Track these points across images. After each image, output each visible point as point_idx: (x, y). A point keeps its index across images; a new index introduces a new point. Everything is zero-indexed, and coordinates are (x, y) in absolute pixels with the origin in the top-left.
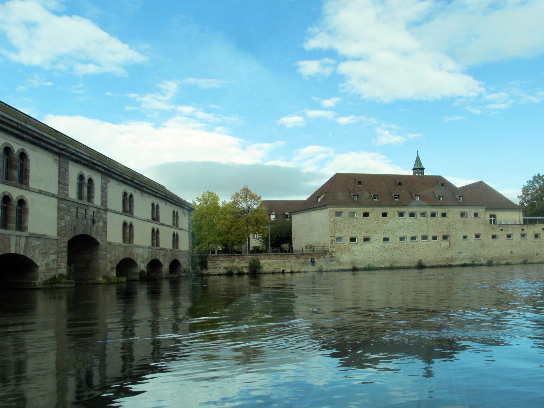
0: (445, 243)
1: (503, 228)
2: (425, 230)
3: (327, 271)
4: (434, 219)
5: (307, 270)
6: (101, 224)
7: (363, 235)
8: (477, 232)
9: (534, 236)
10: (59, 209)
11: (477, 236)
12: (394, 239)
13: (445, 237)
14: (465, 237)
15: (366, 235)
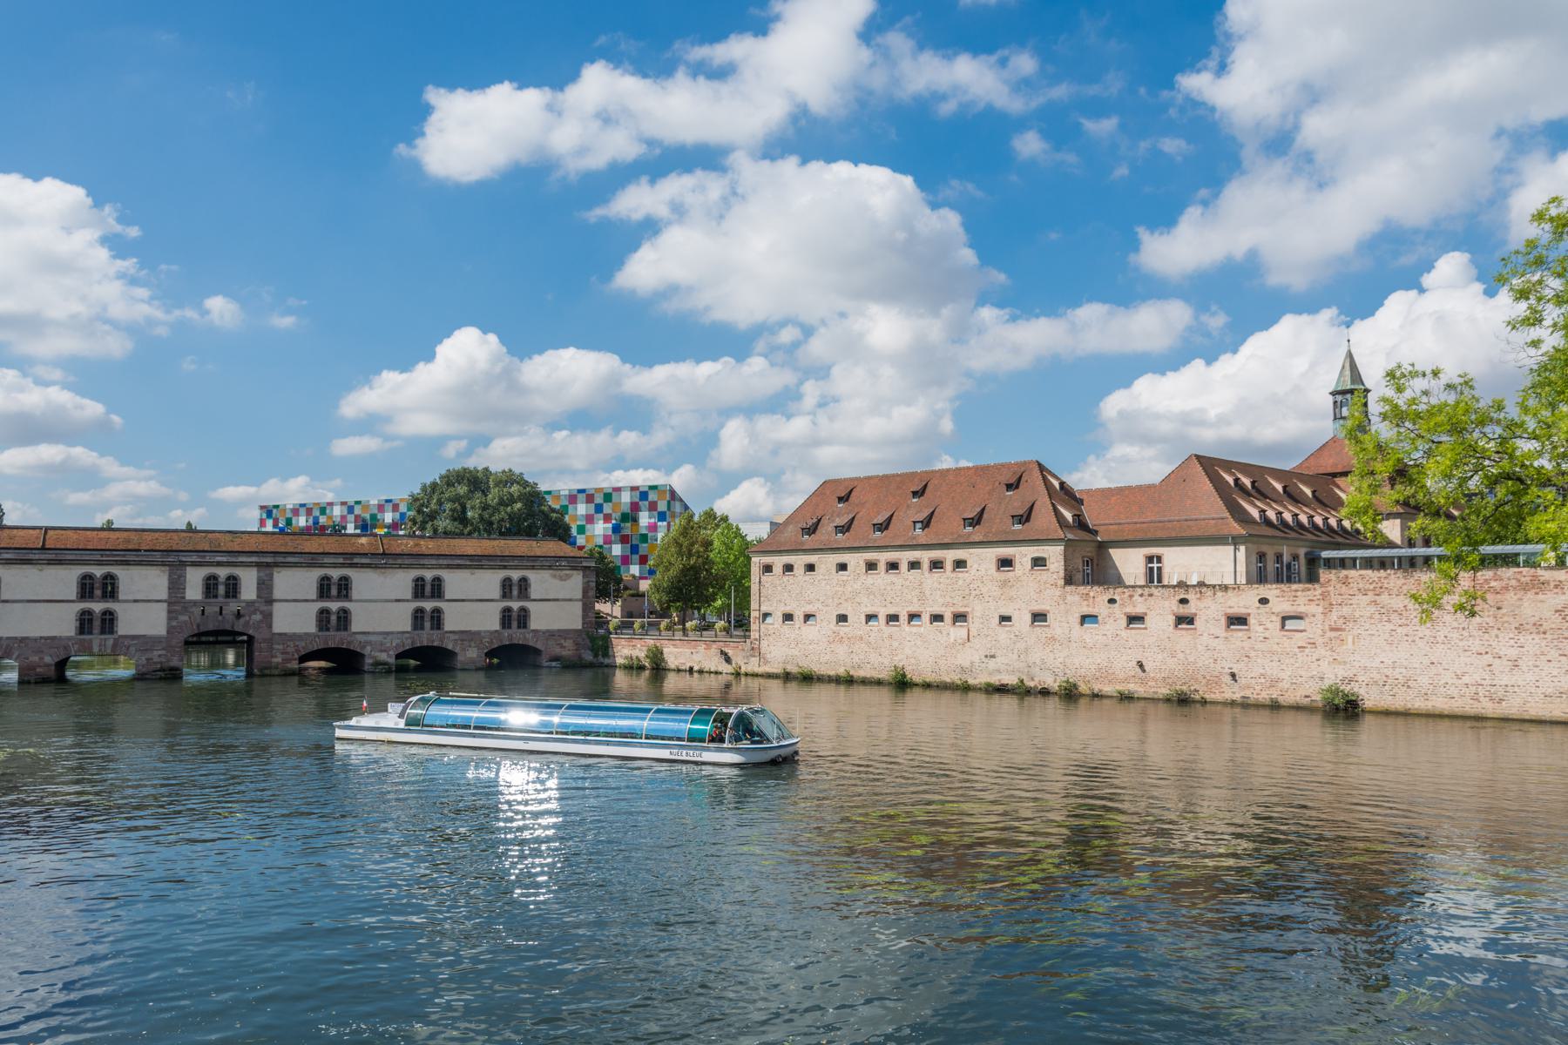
0: (959, 632)
1: (1116, 597)
2: (915, 600)
3: (746, 675)
4: (937, 574)
5: (720, 669)
6: (258, 617)
7: (803, 609)
8: (1037, 608)
9: (1223, 621)
10: (169, 612)
11: (1039, 617)
12: (857, 618)
13: (959, 617)
14: (1005, 619)
15: (809, 609)
